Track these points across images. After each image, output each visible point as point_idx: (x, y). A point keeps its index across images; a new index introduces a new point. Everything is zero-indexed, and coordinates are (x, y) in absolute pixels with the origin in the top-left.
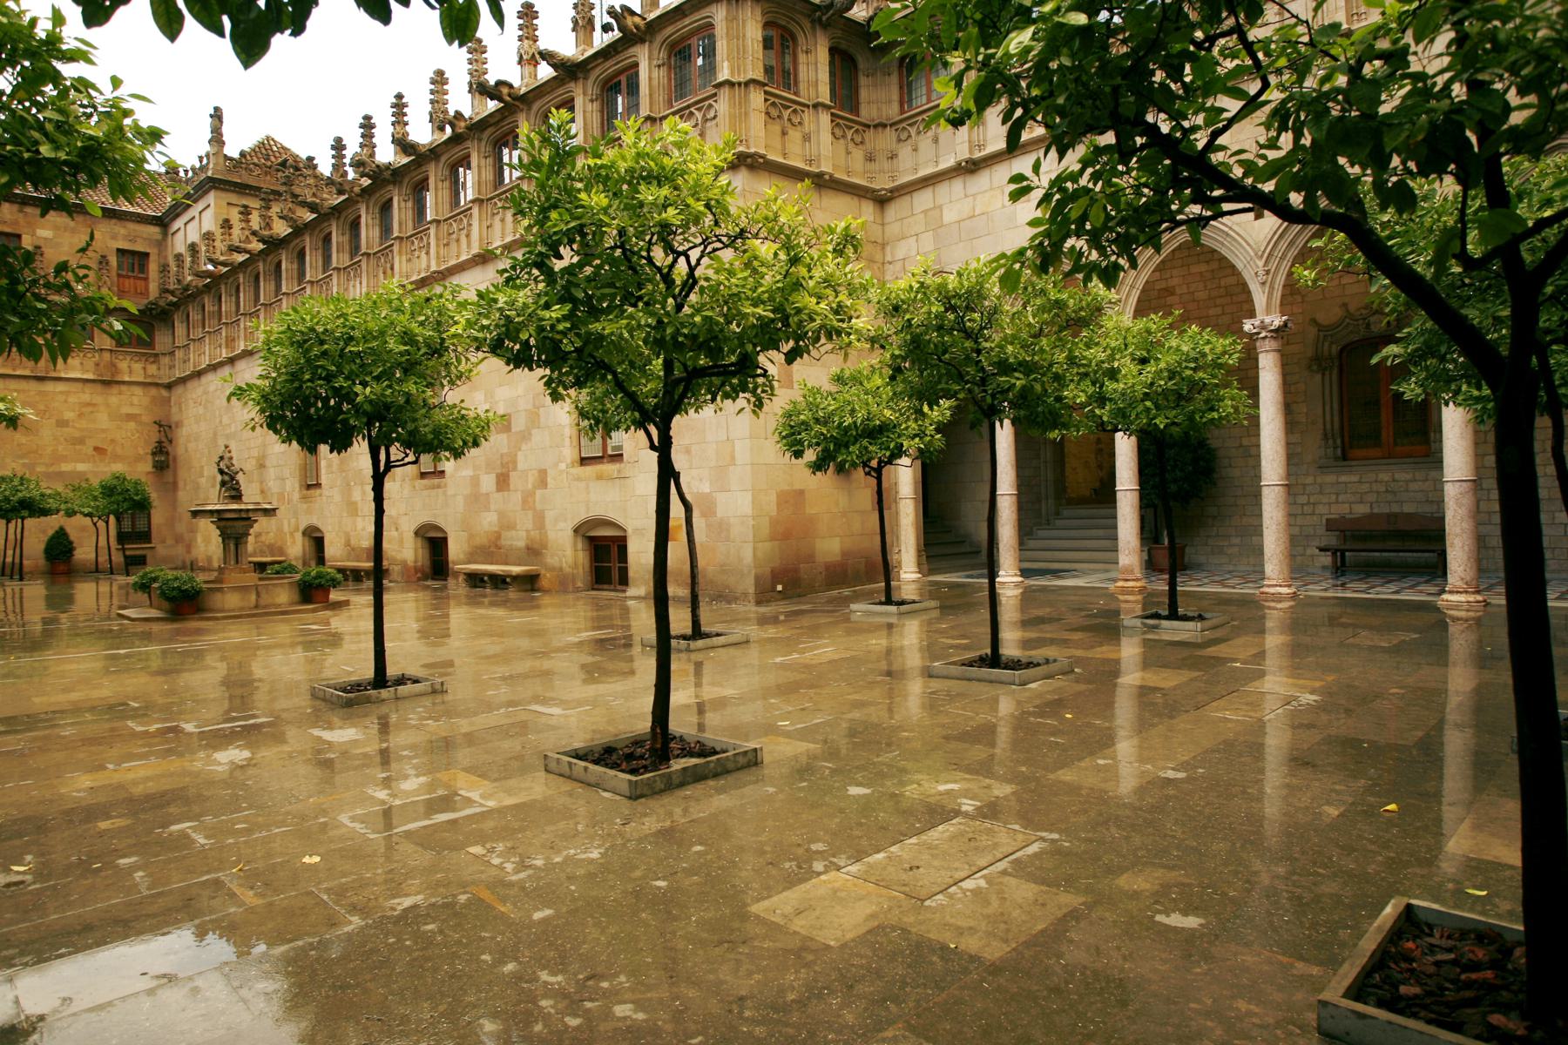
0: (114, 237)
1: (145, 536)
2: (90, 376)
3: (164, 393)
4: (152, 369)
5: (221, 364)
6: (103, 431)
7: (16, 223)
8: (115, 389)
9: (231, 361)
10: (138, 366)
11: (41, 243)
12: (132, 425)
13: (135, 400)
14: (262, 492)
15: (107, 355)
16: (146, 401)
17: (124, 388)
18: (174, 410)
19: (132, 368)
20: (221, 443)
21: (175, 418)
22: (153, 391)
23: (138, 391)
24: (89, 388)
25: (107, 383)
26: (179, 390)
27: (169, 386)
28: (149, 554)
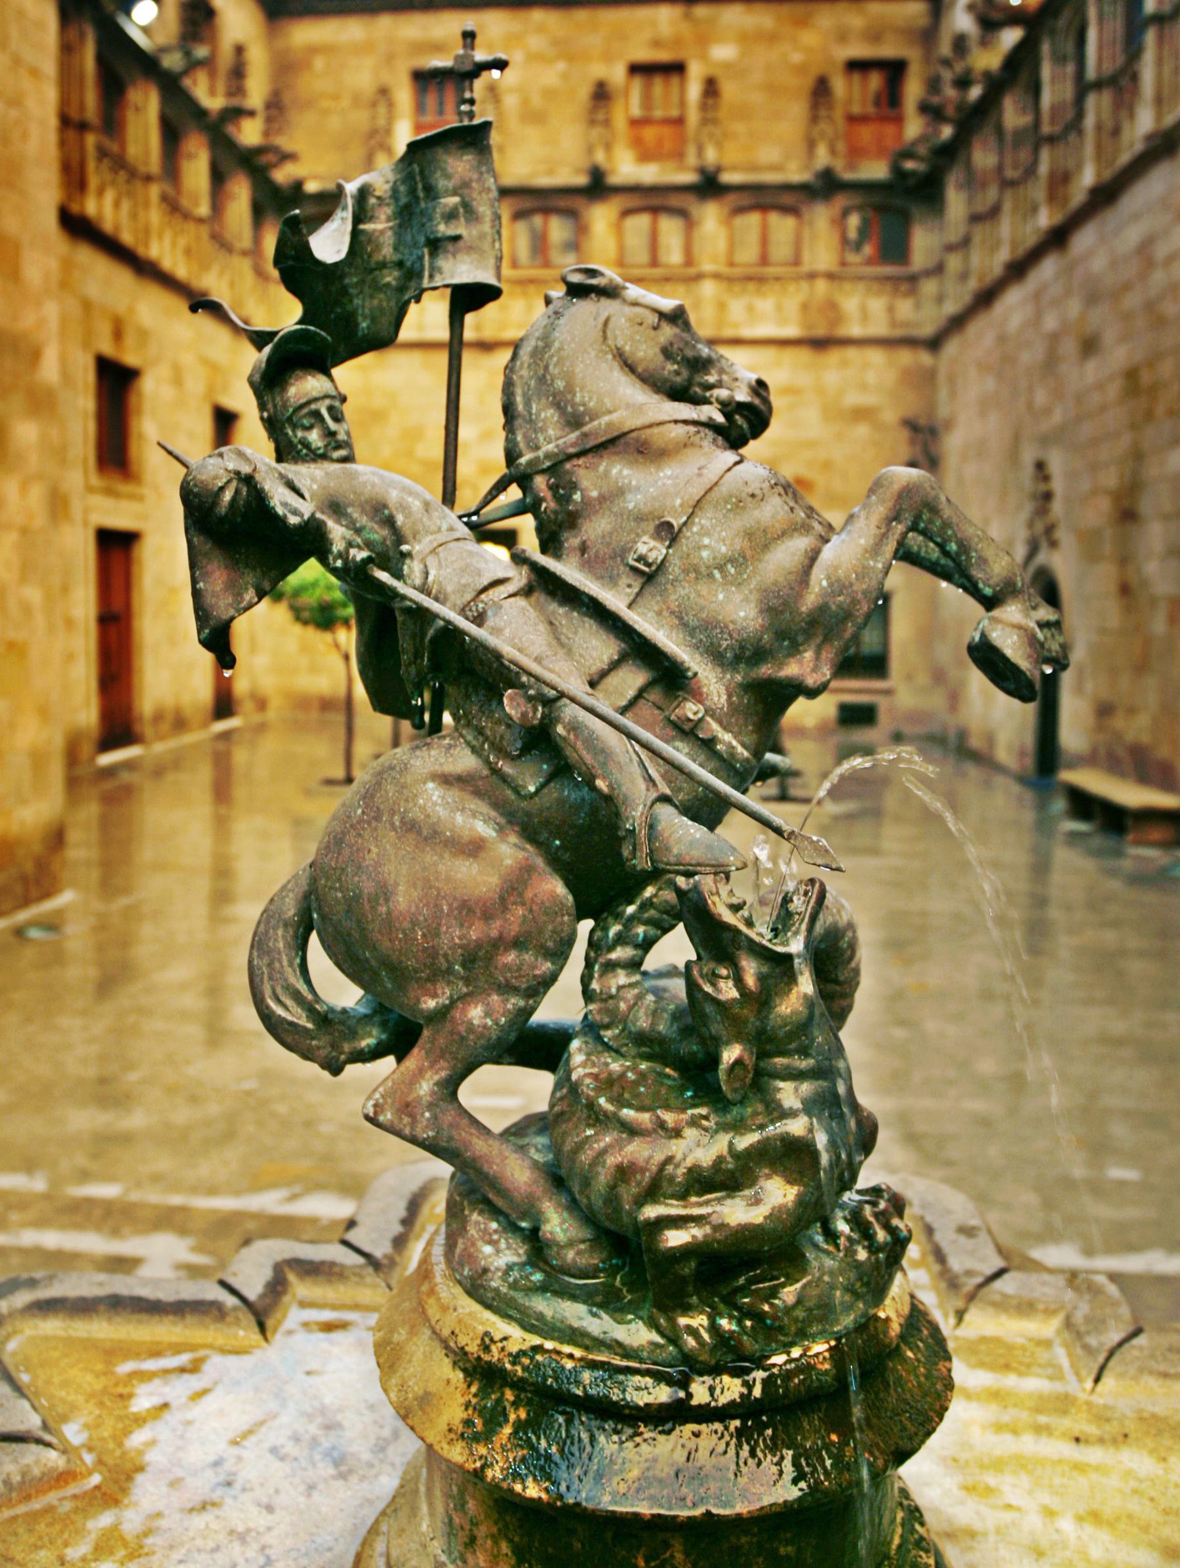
0: (842, 37)
1: (876, 665)
2: (792, 331)
3: (925, 358)
4: (905, 308)
5: (1034, 256)
6: (811, 444)
7: (678, 42)
8: (834, 356)
9: (1058, 238)
10: (877, 305)
11: (717, 72)
12: (862, 430)
13: (871, 377)
14: (1125, 590)
15: (821, 285)
16: (890, 377)
17: (852, 353)
18: (943, 394)
19: (866, 309)
20: (1028, 456)
21: (943, 412)
22: (905, 357)
23: (876, 357)
24: (790, 354)
25: (820, 344)
26: (952, 348)
27: (934, 344)
28: (882, 703)
